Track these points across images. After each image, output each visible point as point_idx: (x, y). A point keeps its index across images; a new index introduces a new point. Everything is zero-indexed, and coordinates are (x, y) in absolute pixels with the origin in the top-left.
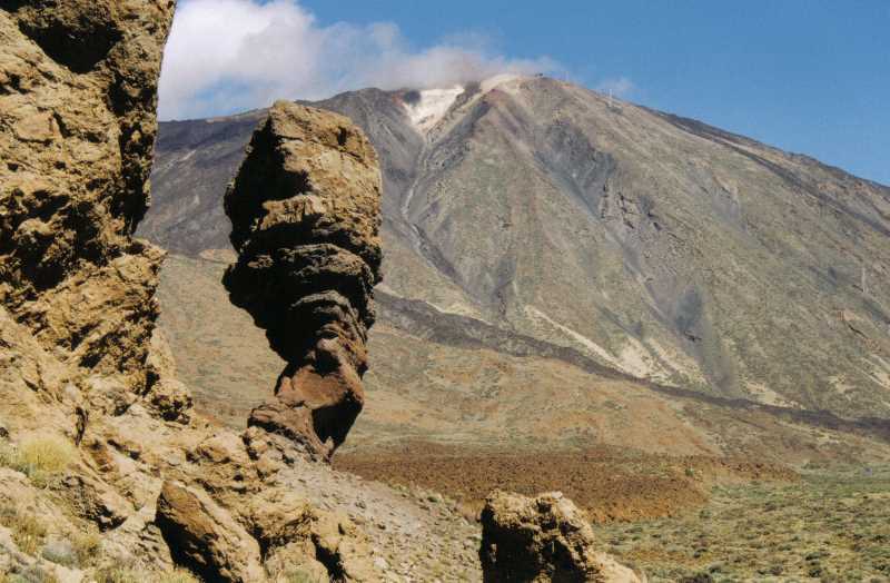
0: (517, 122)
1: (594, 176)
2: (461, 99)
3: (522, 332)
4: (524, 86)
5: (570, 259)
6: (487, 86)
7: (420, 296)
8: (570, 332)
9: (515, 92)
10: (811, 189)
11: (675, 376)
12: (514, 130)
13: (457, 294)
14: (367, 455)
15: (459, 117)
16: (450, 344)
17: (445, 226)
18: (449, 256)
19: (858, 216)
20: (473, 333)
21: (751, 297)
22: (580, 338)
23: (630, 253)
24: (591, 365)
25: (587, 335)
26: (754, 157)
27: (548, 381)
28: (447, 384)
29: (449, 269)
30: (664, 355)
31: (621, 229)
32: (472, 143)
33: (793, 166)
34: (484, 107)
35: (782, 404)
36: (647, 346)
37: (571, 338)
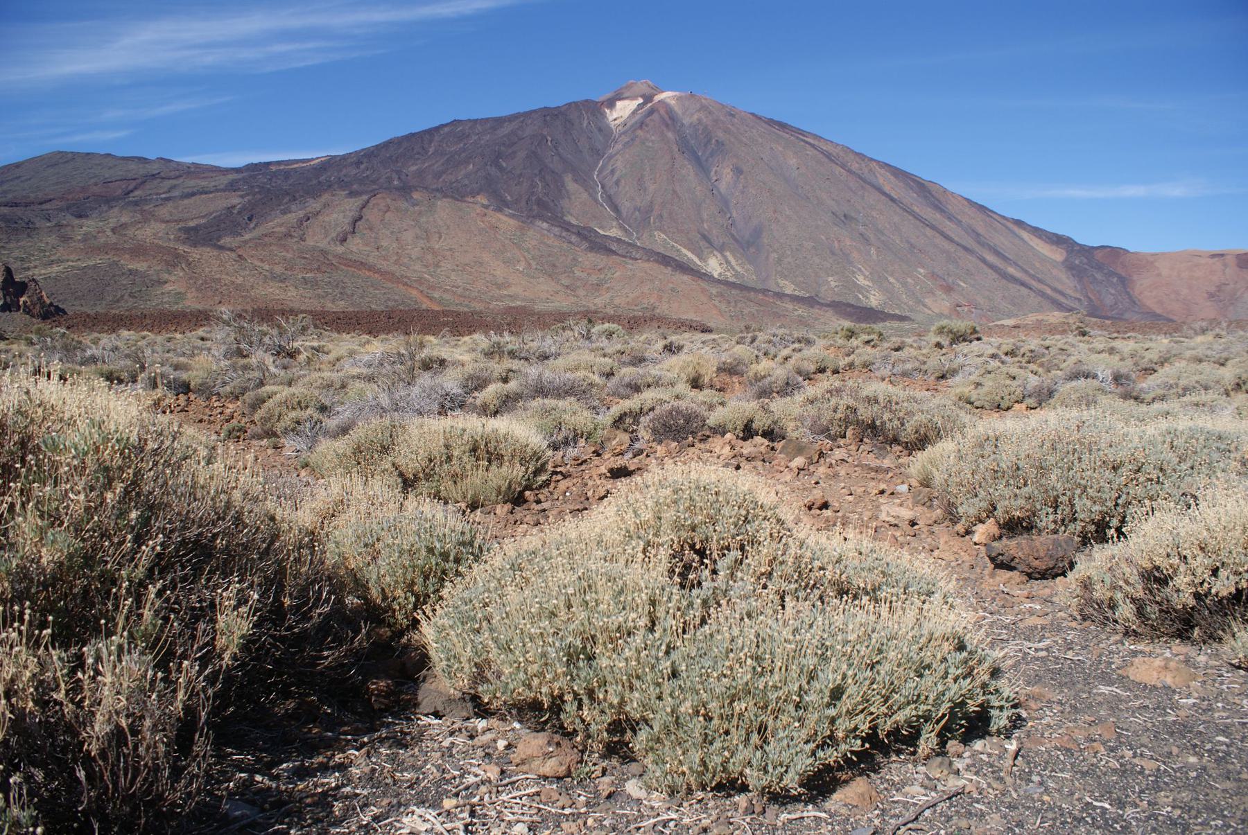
0: (670, 119)
1: (712, 155)
2: (640, 106)
4: (679, 99)
6: (658, 98)
9: (673, 102)
10: (843, 166)
11: (736, 275)
12: (667, 126)
15: (637, 117)
17: (617, 183)
19: (869, 183)
20: (614, 247)
24: (683, 268)
26: (813, 146)
28: (584, 275)
29: (616, 209)
30: (733, 263)
32: (639, 133)
34: (651, 112)
35: (797, 293)
36: (725, 257)
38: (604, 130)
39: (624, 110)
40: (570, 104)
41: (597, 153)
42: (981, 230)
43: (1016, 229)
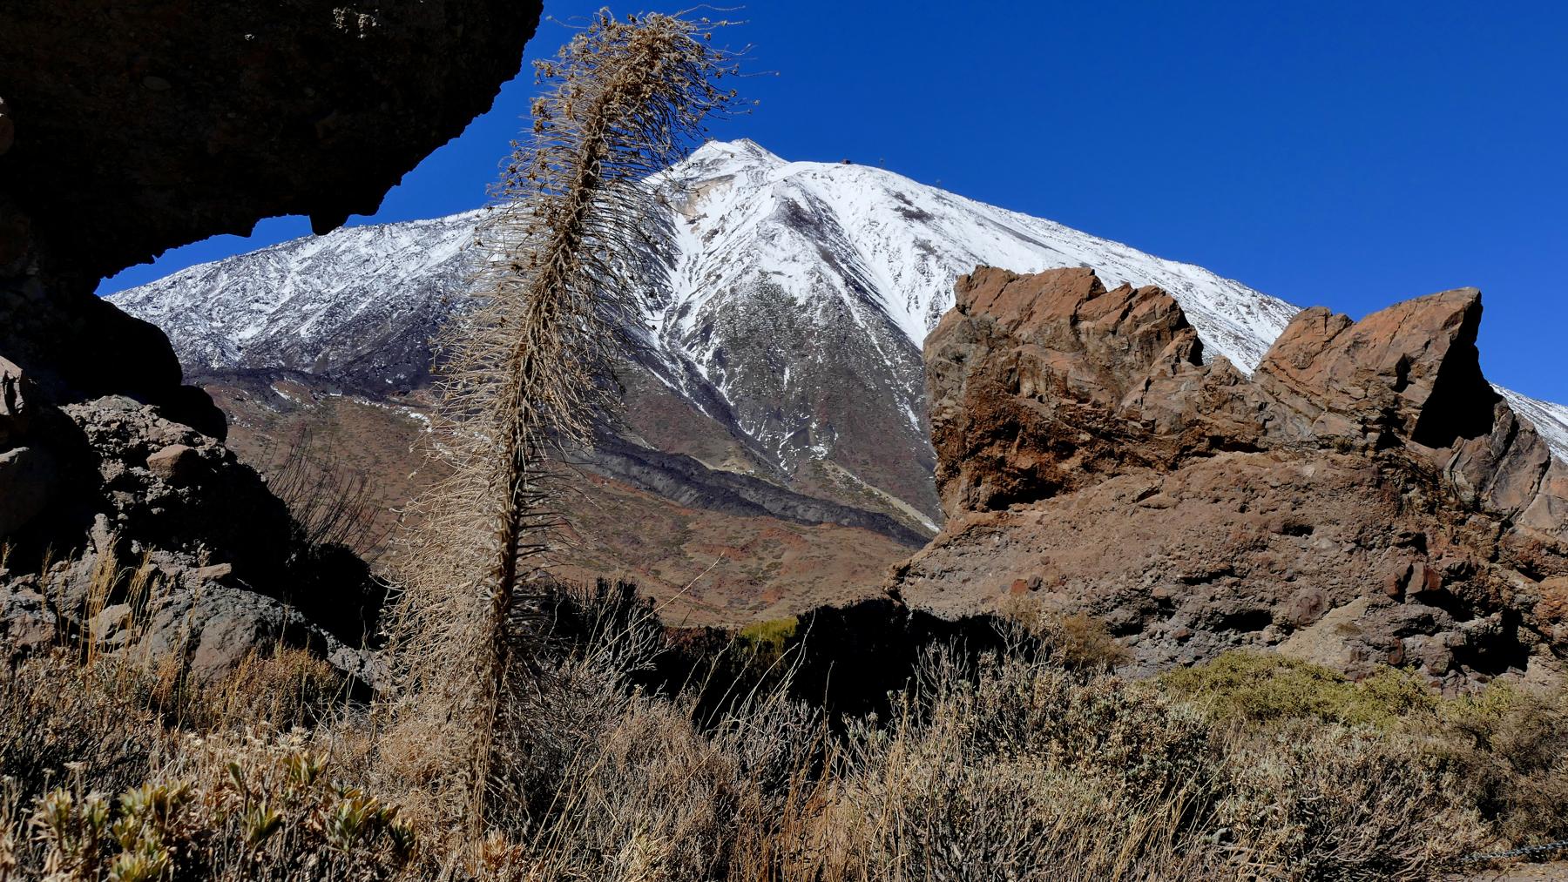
3: (820, 494)
7: (684, 448)
8: (884, 495)
13: (731, 446)
14: (411, 303)
16: (718, 509)
22: (897, 503)
25: (905, 499)
27: (847, 555)
37: (882, 502)
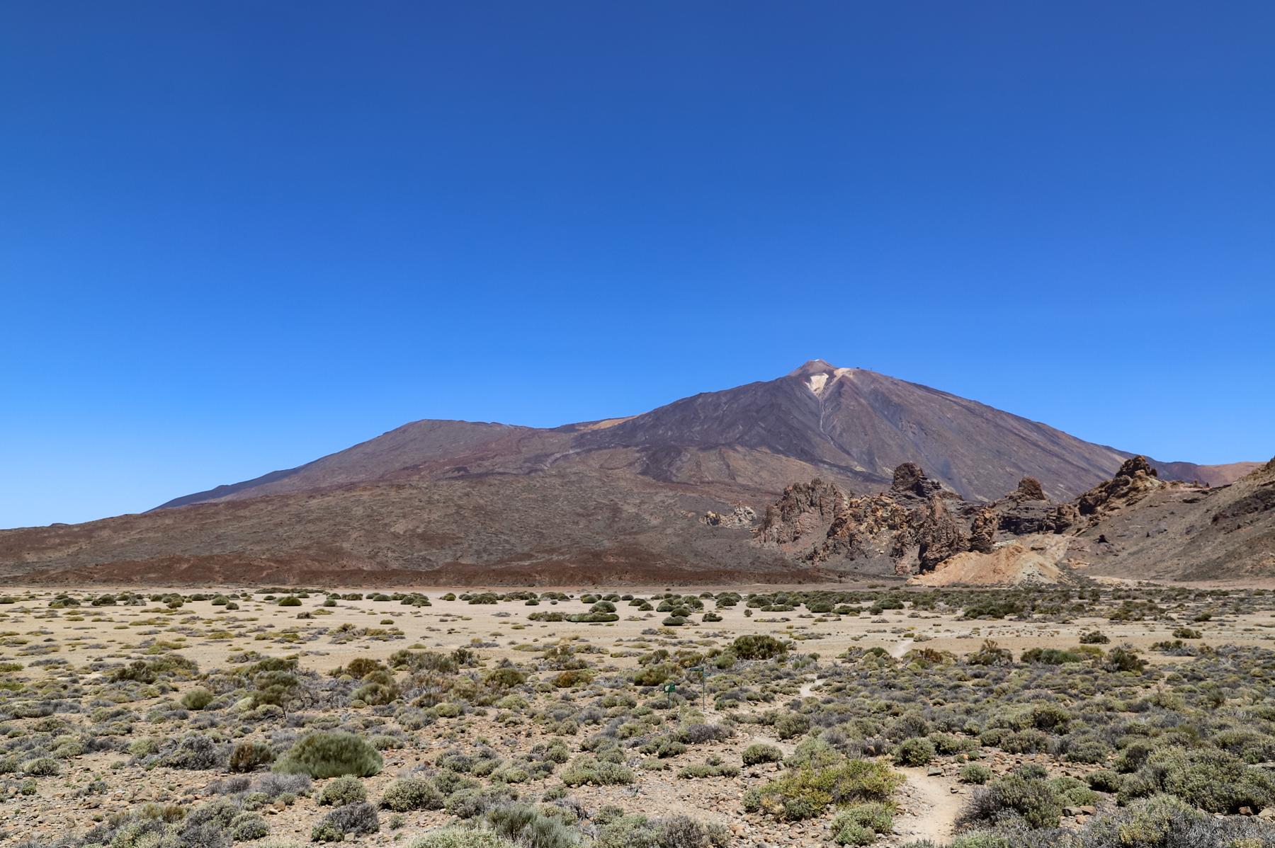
2: (829, 380)
5: (894, 448)
17: (841, 434)
18: (847, 448)
21: (970, 463)
23: (916, 445)
29: (848, 453)
31: (911, 435)
33: (972, 405)
38: (811, 397)
39: (817, 383)
40: (782, 380)
41: (817, 416)
42: (1087, 455)
43: (1109, 453)
